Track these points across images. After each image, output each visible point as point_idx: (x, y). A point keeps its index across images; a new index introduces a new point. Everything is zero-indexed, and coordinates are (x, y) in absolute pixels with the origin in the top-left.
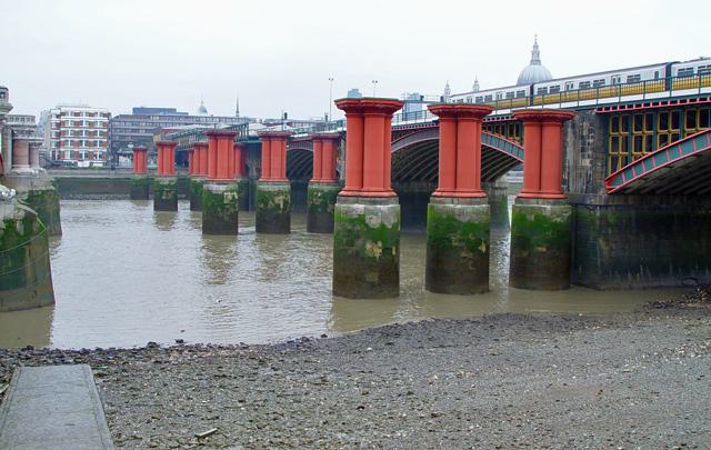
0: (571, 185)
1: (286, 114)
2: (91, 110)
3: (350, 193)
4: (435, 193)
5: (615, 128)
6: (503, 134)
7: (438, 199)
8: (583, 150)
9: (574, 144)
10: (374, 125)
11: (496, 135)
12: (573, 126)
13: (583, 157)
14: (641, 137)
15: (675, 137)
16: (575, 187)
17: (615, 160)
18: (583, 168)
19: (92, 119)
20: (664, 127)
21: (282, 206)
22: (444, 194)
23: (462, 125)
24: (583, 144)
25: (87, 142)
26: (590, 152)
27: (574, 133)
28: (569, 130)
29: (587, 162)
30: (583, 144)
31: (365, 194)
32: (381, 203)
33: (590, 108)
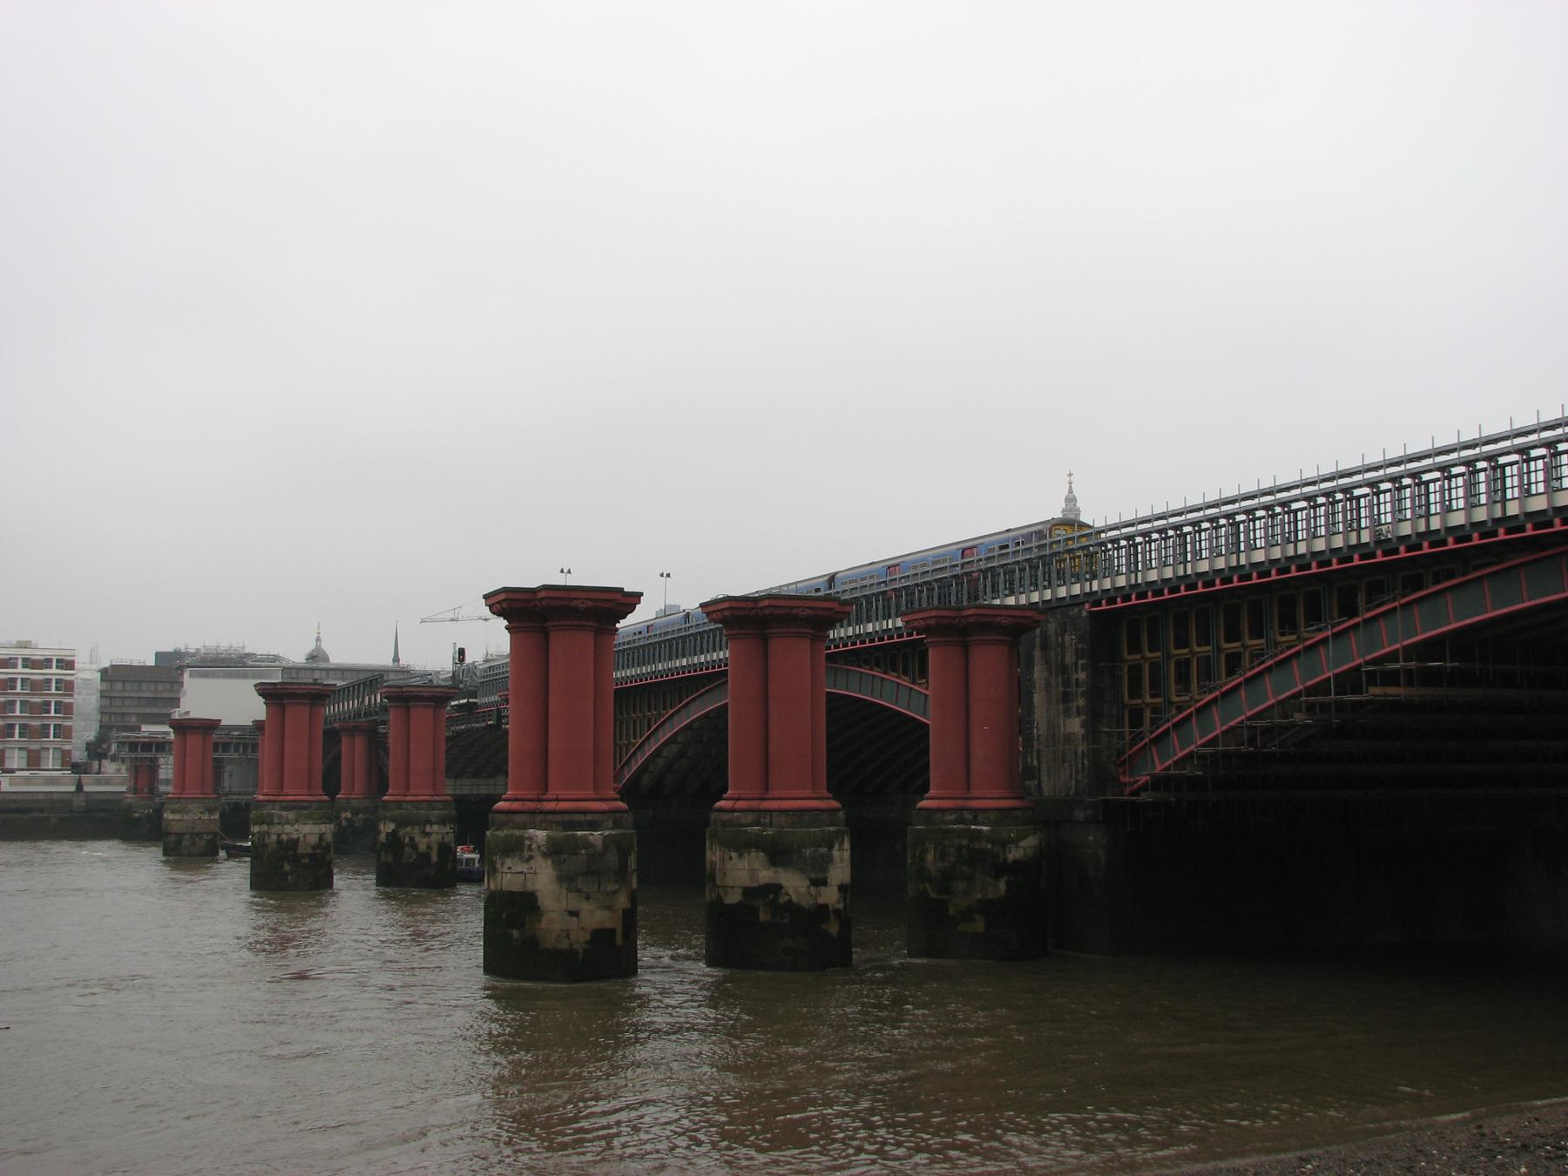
0: (1044, 778)
1: (462, 652)
2: (37, 654)
3: (516, 805)
4: (721, 804)
5: (1135, 647)
6: (905, 674)
7: (726, 817)
8: (1066, 698)
9: (1048, 685)
10: (570, 648)
11: (891, 677)
12: (1045, 647)
13: (1067, 714)
14: (1187, 662)
15: (1258, 655)
16: (1056, 782)
17: (1136, 718)
18: (1068, 738)
19: (37, 675)
20: (1233, 635)
21: (434, 858)
22: (741, 804)
23: (777, 646)
24: (1066, 683)
25: (23, 727)
26: (1081, 702)
27: (1047, 662)
28: (1037, 654)
29: (1075, 726)
30: (1066, 683)
31: (551, 806)
32: (593, 826)
33: (1075, 601)
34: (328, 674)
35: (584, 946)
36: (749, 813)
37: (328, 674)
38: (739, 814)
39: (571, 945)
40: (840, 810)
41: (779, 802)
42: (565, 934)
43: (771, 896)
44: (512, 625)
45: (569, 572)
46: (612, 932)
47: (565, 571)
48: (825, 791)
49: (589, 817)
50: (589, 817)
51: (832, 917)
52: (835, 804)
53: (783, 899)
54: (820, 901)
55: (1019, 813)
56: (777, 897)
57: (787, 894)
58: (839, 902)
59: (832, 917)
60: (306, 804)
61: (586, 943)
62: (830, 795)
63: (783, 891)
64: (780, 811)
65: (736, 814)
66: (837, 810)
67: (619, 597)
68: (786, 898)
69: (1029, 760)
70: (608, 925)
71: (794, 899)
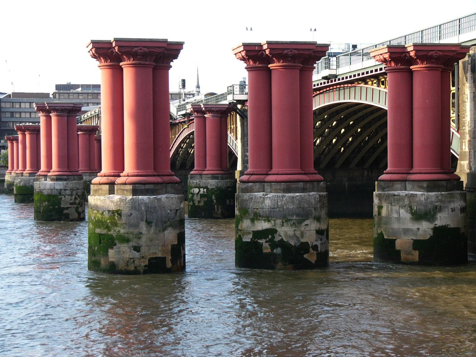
22: (253, 178)
34: (69, 96)
35: (144, 268)
36: (258, 183)
37: (69, 96)
38: (252, 184)
39: (136, 267)
40: (322, 181)
41: (276, 176)
42: (132, 260)
43: (270, 237)
44: (101, 64)
45: (251, 29)
46: (164, 259)
47: (249, 29)
48: (313, 169)
49: (147, 187)
50: (147, 187)
51: (311, 250)
52: (319, 177)
53: (277, 239)
54: (303, 240)
55: (444, 183)
56: (273, 237)
57: (280, 235)
58: (316, 241)
59: (311, 250)
60: (65, 177)
61: (145, 266)
62: (316, 172)
63: (278, 233)
64: (276, 182)
65: (250, 184)
66: (319, 181)
67: (164, 45)
68: (280, 238)
69: (464, 147)
70: (160, 255)
71: (285, 240)
